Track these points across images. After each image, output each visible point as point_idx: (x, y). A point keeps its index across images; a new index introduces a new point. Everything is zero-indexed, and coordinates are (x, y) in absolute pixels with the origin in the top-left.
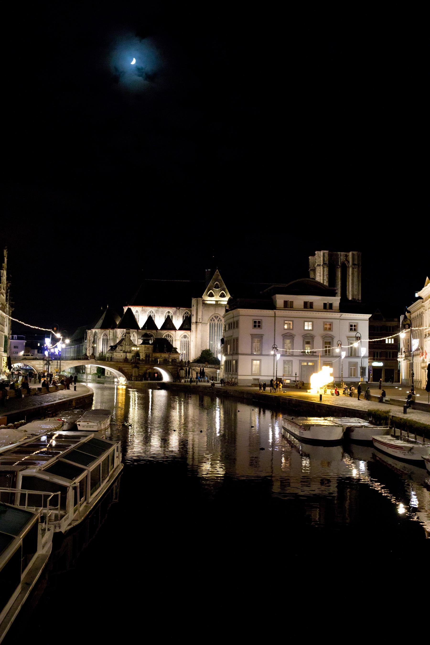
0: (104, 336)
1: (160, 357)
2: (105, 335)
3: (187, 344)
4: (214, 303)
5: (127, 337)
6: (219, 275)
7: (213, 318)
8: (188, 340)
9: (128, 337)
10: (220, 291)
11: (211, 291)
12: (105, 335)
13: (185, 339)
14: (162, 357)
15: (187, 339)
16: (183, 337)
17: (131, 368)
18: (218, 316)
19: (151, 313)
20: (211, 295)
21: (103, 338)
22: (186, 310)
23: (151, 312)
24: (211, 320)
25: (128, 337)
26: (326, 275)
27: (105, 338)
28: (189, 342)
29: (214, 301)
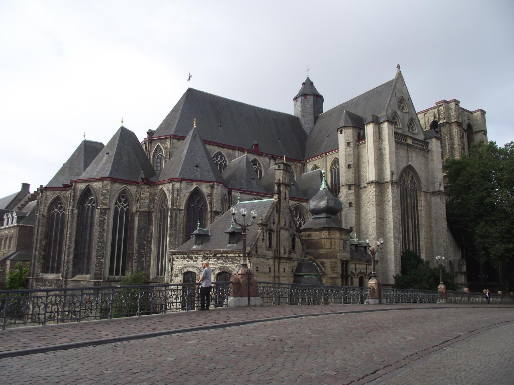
0: (120, 202)
1: (354, 271)
2: (123, 200)
12: (123, 200)
14: (357, 272)
21: (116, 208)
25: (285, 198)
27: (122, 208)
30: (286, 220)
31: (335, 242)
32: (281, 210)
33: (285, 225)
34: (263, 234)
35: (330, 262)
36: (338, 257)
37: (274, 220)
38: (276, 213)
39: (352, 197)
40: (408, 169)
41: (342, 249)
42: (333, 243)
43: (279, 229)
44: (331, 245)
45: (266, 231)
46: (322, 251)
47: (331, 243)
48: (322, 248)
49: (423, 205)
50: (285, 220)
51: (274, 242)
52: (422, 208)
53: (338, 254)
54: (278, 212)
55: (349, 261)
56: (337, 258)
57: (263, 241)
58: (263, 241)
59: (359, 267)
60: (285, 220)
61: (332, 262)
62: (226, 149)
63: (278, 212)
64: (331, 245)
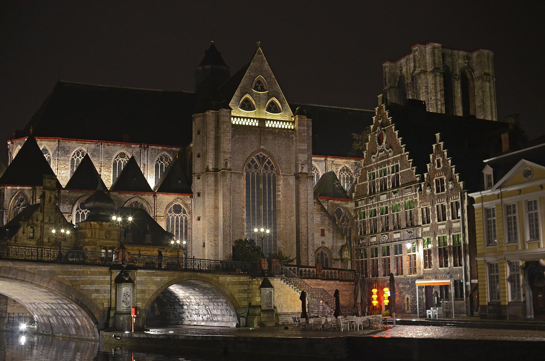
3: (182, 226)
4: (256, 123)
5: (47, 199)
6: (264, 61)
7: (253, 161)
8: (184, 218)
9: (50, 201)
10: (266, 97)
11: (247, 96)
13: (177, 215)
15: (182, 214)
16: (172, 209)
17: (108, 287)
18: (264, 156)
19: (80, 155)
20: (247, 106)
22: (163, 150)
23: (81, 153)
24: (249, 166)
26: (441, 91)
28: (186, 221)
29: (257, 119)
30: (51, 218)
31: (95, 232)
32: (45, 211)
33: (49, 221)
34: (24, 228)
35: (91, 248)
36: (98, 244)
37: (37, 218)
38: (40, 213)
39: (200, 187)
40: (262, 153)
41: (104, 237)
42: (93, 233)
43: (42, 224)
44: (92, 235)
45: (28, 226)
46: (87, 240)
47: (92, 234)
48: (86, 238)
49: (280, 189)
50: (49, 217)
51: (38, 235)
52: (280, 193)
53: (98, 242)
54: (43, 212)
55: (115, 247)
56: (96, 245)
57: (23, 234)
58: (23, 234)
59: (147, 253)
60: (49, 217)
61: (92, 248)
62: (87, 145)
63: (43, 212)
64: (92, 235)
